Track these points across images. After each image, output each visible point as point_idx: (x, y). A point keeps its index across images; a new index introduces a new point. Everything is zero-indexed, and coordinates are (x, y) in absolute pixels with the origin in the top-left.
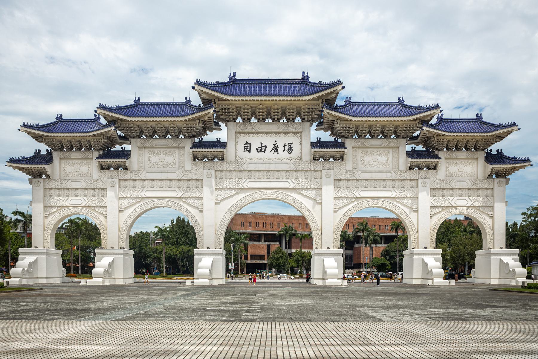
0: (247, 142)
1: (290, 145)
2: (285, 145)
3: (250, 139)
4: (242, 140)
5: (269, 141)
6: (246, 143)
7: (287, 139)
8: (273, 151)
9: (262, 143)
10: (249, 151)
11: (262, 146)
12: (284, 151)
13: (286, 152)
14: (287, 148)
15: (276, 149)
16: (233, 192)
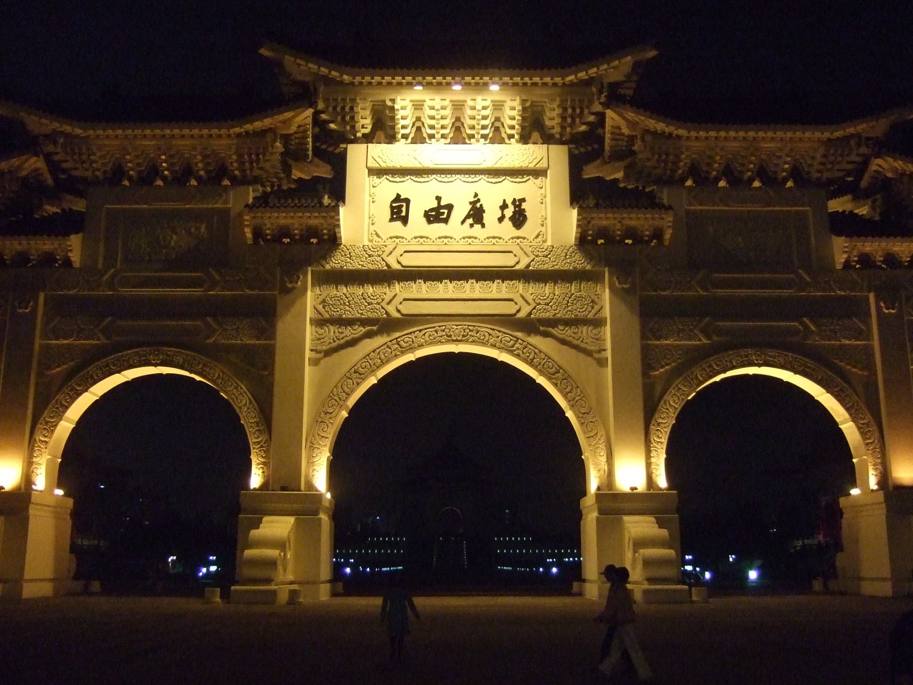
0: (398, 196)
1: (518, 204)
2: (504, 206)
3: (407, 188)
4: (388, 189)
5: (458, 194)
6: (398, 198)
7: (509, 190)
8: (470, 221)
9: (438, 199)
10: (405, 220)
11: (440, 207)
12: (501, 220)
13: (507, 223)
14: (509, 212)
15: (476, 214)
16: (362, 330)
